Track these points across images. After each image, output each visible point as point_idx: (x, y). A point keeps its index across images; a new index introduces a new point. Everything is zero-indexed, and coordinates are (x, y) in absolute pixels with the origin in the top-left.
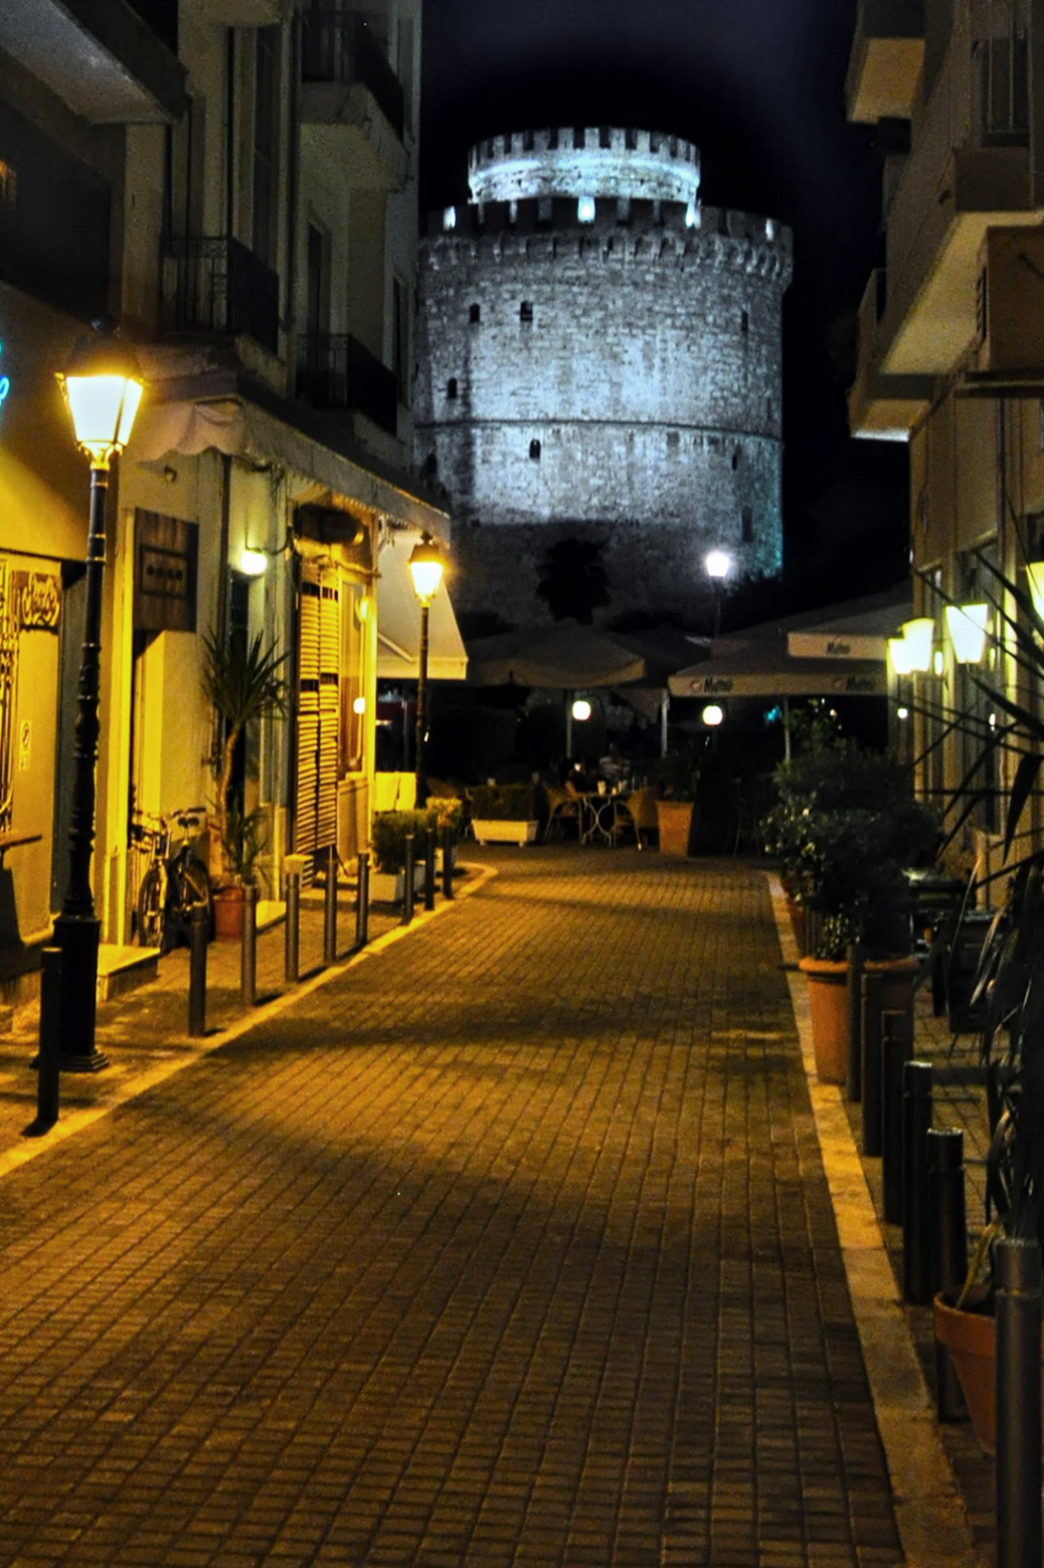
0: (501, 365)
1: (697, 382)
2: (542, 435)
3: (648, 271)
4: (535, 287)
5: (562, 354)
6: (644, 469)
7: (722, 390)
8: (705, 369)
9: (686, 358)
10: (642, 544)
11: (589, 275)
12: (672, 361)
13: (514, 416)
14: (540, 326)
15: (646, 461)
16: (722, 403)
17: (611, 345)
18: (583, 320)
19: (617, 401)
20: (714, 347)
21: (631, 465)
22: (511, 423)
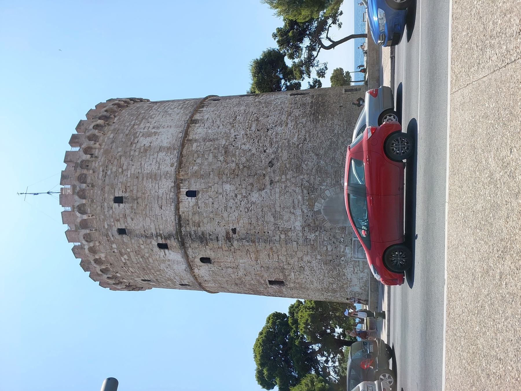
0: (146, 215)
2: (184, 190)
4: (106, 195)
5: (140, 179)
10: (248, 133)
13: (173, 208)
14: (126, 192)
17: (140, 152)
18: (125, 167)
19: (169, 149)
22: (177, 208)
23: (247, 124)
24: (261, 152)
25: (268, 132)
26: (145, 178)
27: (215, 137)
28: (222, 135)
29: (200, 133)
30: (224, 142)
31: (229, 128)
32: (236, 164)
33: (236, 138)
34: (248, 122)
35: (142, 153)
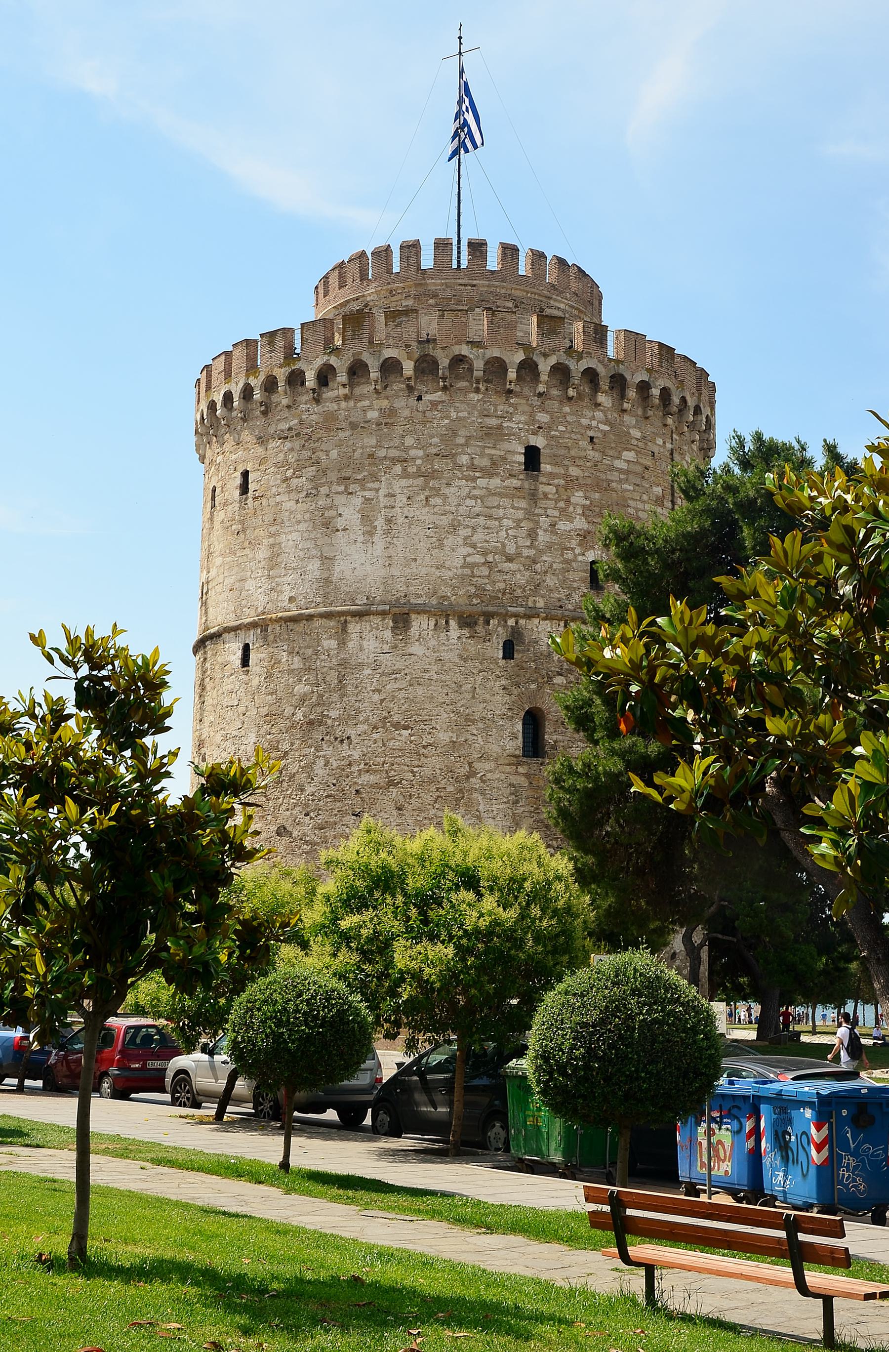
1: (441, 546)
2: (251, 637)
3: (370, 407)
5: (273, 529)
6: (360, 666)
7: (485, 554)
8: (454, 528)
9: (422, 513)
10: (355, 768)
11: (301, 423)
12: (401, 520)
14: (255, 498)
15: (362, 657)
16: (485, 571)
18: (294, 482)
19: (327, 581)
20: (469, 496)
21: (343, 664)
23: (380, 760)
24: (307, 805)
25: (353, 815)
26: (271, 540)
27: (350, 688)
28: (352, 707)
29: (361, 649)
30: (334, 714)
31: (371, 718)
32: (286, 753)
33: (342, 741)
34: (384, 762)
35: (323, 515)
